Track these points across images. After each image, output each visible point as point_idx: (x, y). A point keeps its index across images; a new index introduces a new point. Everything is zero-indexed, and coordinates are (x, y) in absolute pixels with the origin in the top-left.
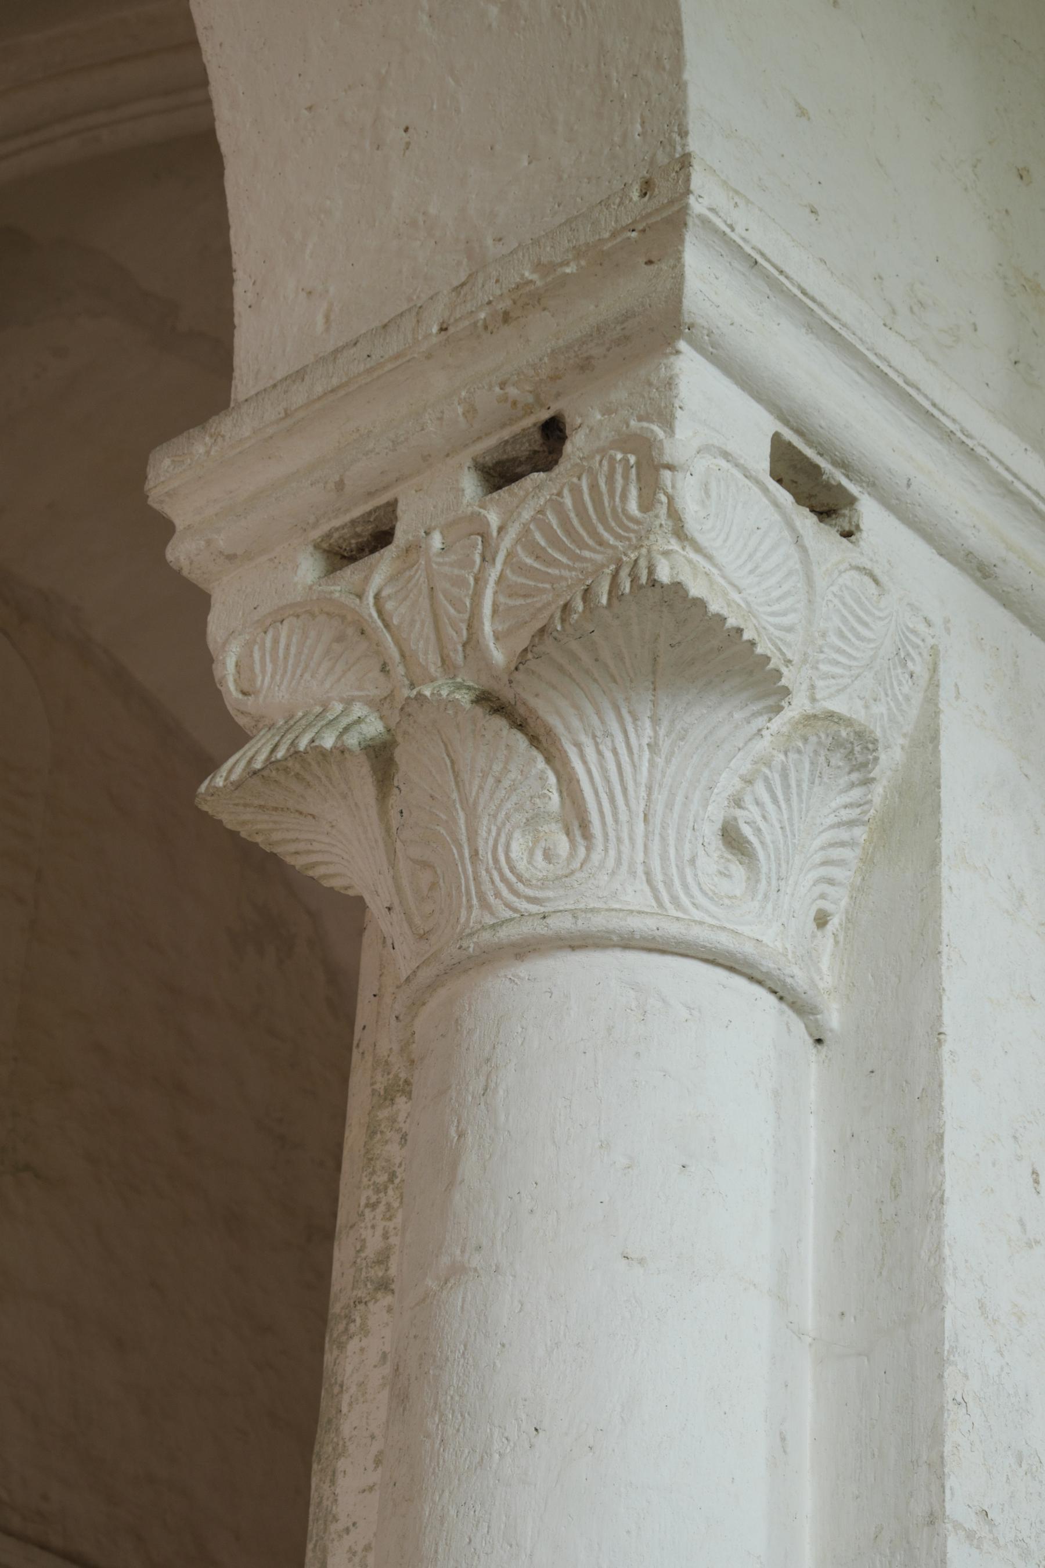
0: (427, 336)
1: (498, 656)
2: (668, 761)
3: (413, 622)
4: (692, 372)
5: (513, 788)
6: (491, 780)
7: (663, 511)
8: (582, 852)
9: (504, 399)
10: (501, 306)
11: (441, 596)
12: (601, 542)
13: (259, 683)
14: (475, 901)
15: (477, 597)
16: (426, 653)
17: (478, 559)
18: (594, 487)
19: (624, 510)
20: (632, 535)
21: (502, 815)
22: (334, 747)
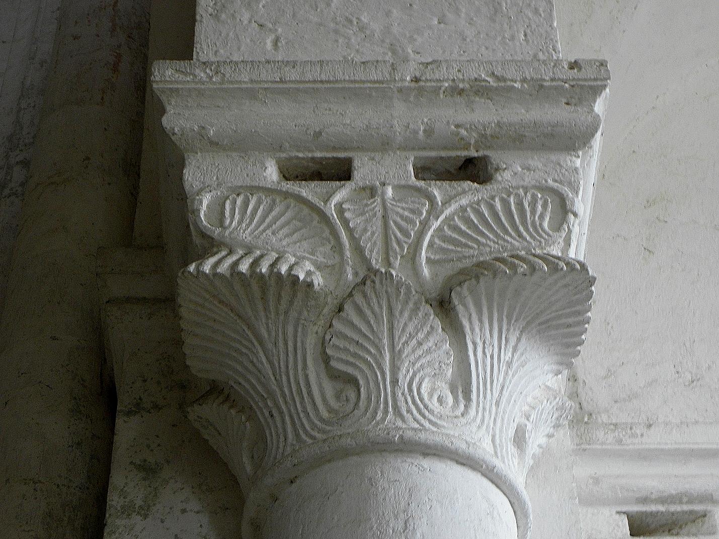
0: (402, 80)
1: (426, 271)
2: (513, 376)
3: (365, 230)
5: (429, 351)
6: (414, 341)
9: (458, 134)
10: (461, 86)
11: (392, 223)
12: (520, 235)
13: (228, 222)
14: (390, 409)
16: (371, 251)
18: (520, 205)
19: (541, 225)
20: (543, 240)
21: (418, 365)
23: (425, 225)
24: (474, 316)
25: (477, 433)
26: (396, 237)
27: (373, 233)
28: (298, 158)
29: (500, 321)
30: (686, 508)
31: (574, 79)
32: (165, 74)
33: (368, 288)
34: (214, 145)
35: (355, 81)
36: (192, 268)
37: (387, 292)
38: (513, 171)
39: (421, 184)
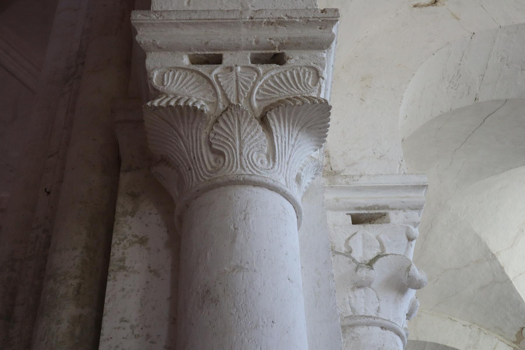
0: (245, 18)
1: (255, 105)
3: (228, 86)
6: (250, 136)
7: (318, 87)
8: (271, 165)
9: (270, 42)
10: (272, 21)
11: (240, 83)
12: (298, 88)
13: (165, 83)
14: (239, 166)
15: (253, 88)
16: (231, 96)
17: (255, 79)
18: (298, 74)
21: (251, 146)
22: (200, 109)
23: (255, 84)
24: (277, 124)
25: (279, 176)
26: (242, 90)
27: (232, 88)
28: (197, 54)
29: (289, 126)
30: (377, 211)
31: (323, 17)
32: (137, 16)
33: (229, 112)
34: (160, 48)
35: (224, 19)
36: (149, 104)
37: (237, 114)
38: (296, 59)
39: (253, 65)
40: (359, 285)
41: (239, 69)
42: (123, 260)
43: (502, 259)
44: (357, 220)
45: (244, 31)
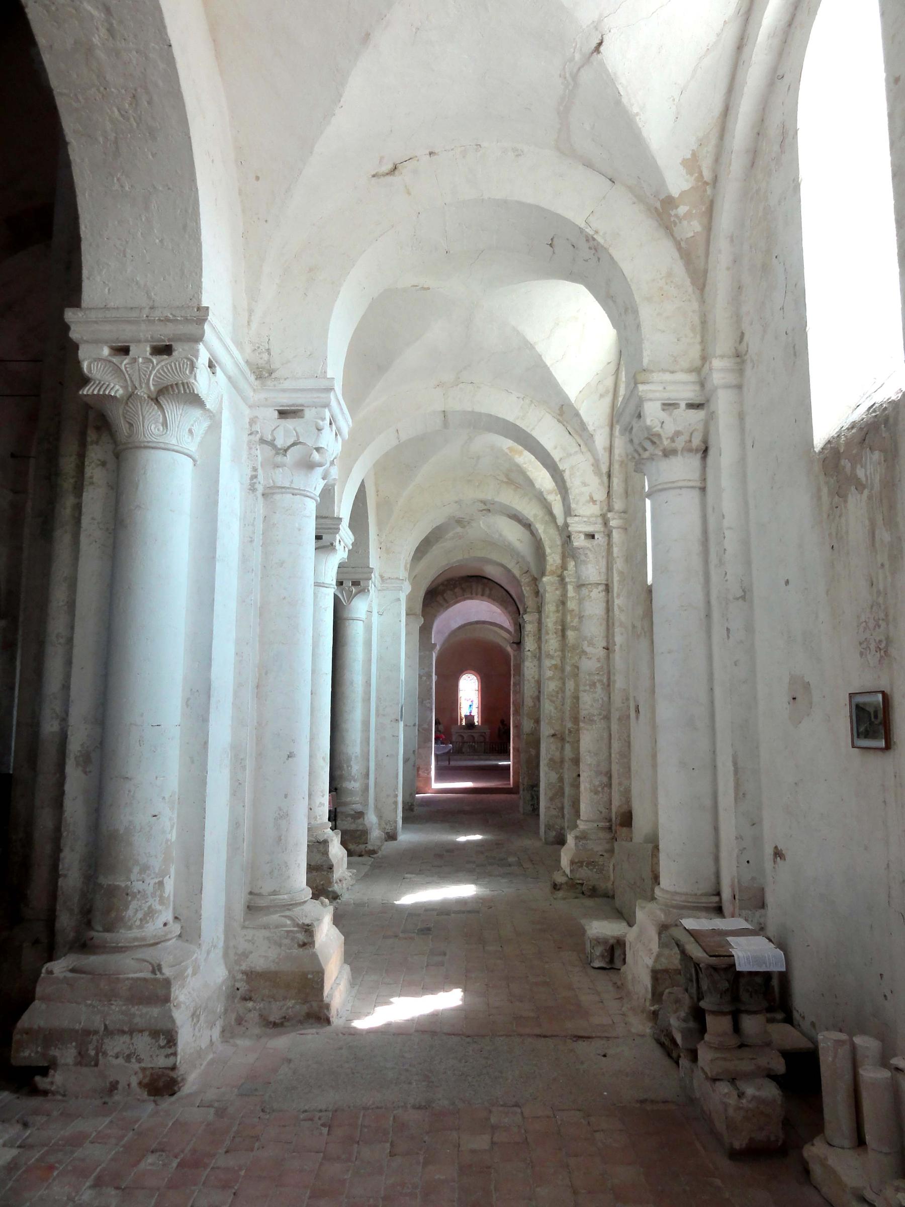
1: (152, 388)
4: (201, 347)
15: (150, 376)
23: (151, 372)
32: (70, 315)
34: (87, 342)
38: (179, 350)
39: (150, 357)
40: (277, 466)
41: (140, 360)
42: (91, 477)
43: (540, 348)
44: (283, 414)
45: (143, 327)
